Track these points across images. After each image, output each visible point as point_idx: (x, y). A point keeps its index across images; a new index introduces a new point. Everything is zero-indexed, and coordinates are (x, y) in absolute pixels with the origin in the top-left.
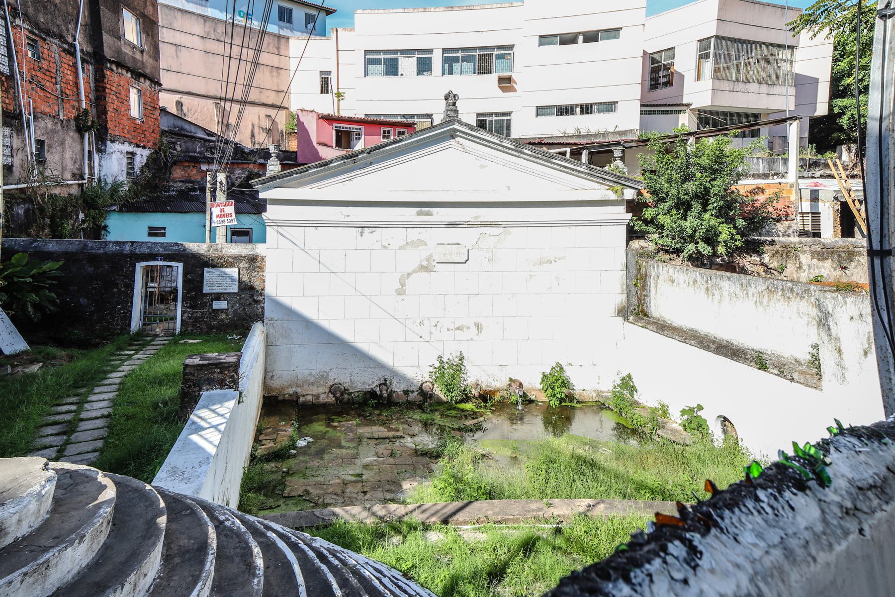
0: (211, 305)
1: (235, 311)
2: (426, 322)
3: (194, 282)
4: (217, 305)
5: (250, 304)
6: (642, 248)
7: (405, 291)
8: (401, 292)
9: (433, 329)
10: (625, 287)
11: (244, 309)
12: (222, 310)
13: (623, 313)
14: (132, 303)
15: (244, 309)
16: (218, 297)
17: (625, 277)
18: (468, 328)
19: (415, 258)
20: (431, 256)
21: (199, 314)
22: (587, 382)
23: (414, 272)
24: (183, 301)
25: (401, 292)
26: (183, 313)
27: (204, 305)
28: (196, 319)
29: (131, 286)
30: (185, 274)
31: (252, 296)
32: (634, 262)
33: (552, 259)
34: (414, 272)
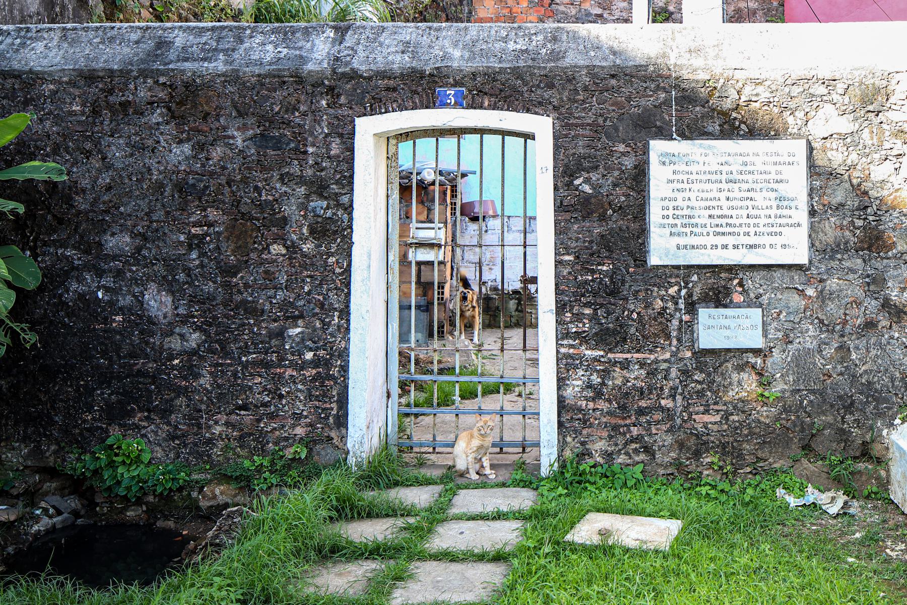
0: (689, 327)
1: (800, 362)
3: (604, 219)
4: (717, 329)
5: (870, 325)
11: (843, 349)
12: (738, 356)
14: (345, 313)
15: (843, 349)
16: (719, 285)
21: (636, 374)
24: (561, 308)
26: (566, 366)
27: (656, 330)
28: (624, 401)
29: (335, 232)
30: (565, 173)
31: (875, 283)
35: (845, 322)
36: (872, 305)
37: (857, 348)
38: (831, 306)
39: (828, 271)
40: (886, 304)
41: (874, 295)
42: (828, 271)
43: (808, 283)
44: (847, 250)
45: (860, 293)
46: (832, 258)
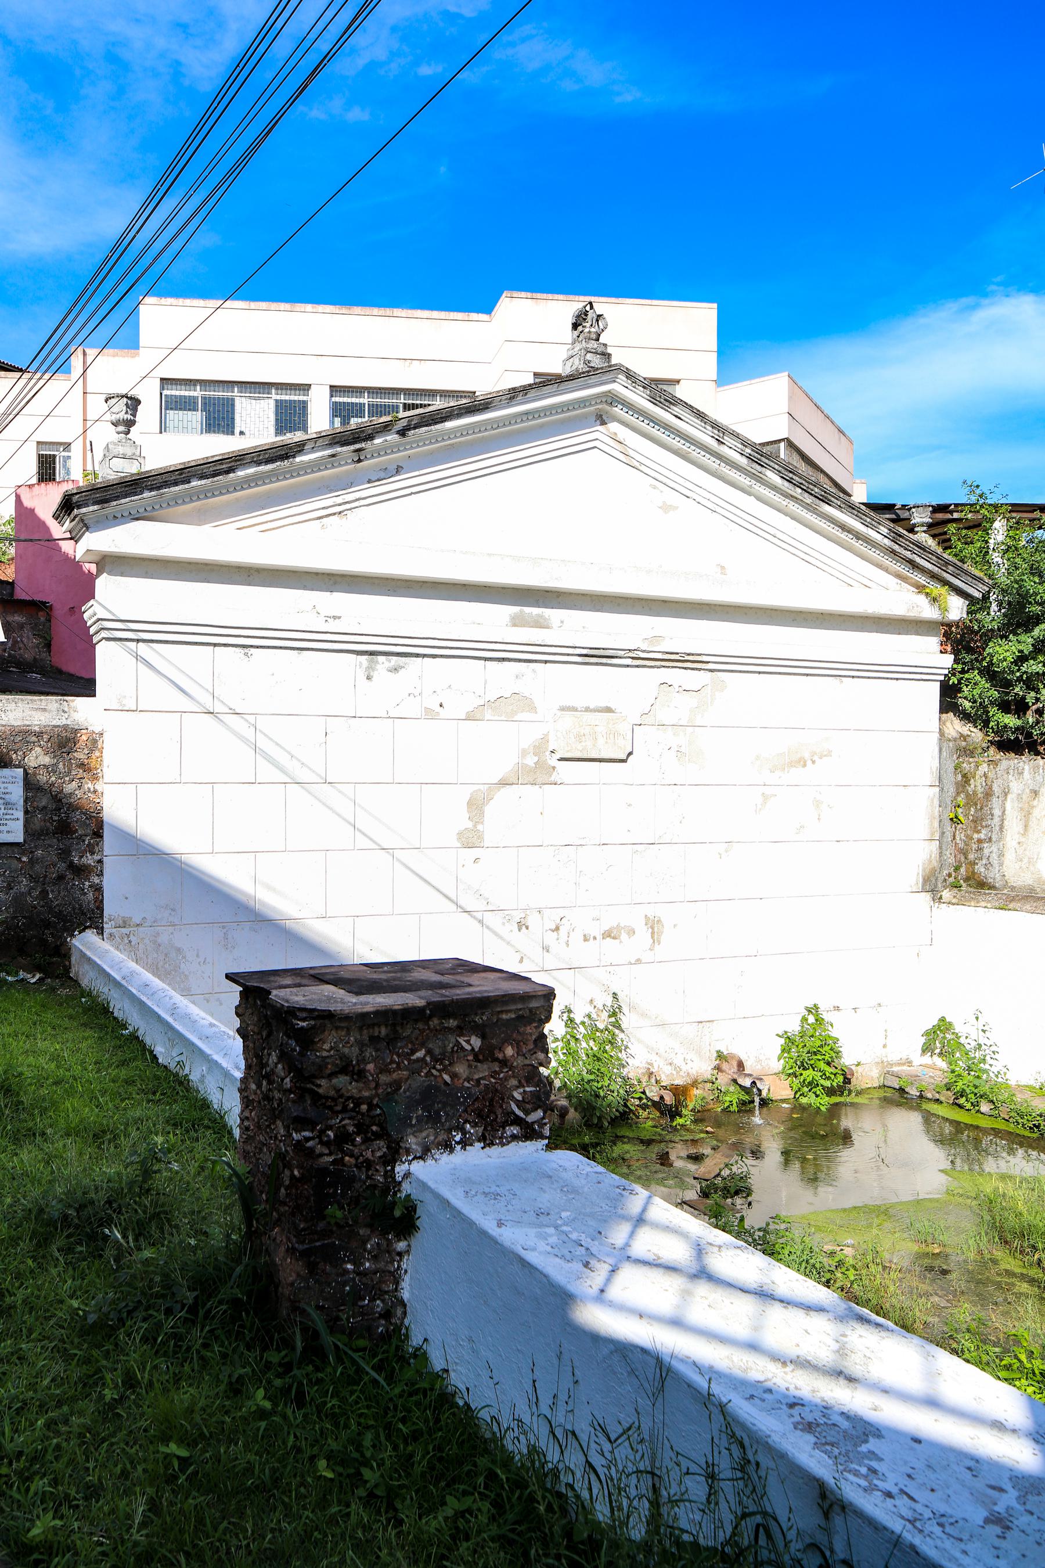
2: (533, 920)
5: (61, 878)
6: (962, 735)
7: (481, 837)
8: (470, 840)
9: (550, 938)
10: (936, 824)
11: (44, 893)
13: (931, 886)
15: (44, 893)
17: (936, 802)
18: (631, 932)
19: (500, 747)
20: (545, 739)
22: (876, 1045)
23: (504, 783)
25: (470, 840)
31: (65, 854)
32: (950, 766)
33: (807, 756)
34: (504, 783)
35: (45, 876)
36: (62, 866)
37: (52, 891)
38: (37, 867)
39: (36, 847)
40: (71, 866)
41: (63, 860)
42: (36, 847)
43: (23, 853)
44: (47, 834)
45: (55, 859)
46: (38, 839)
